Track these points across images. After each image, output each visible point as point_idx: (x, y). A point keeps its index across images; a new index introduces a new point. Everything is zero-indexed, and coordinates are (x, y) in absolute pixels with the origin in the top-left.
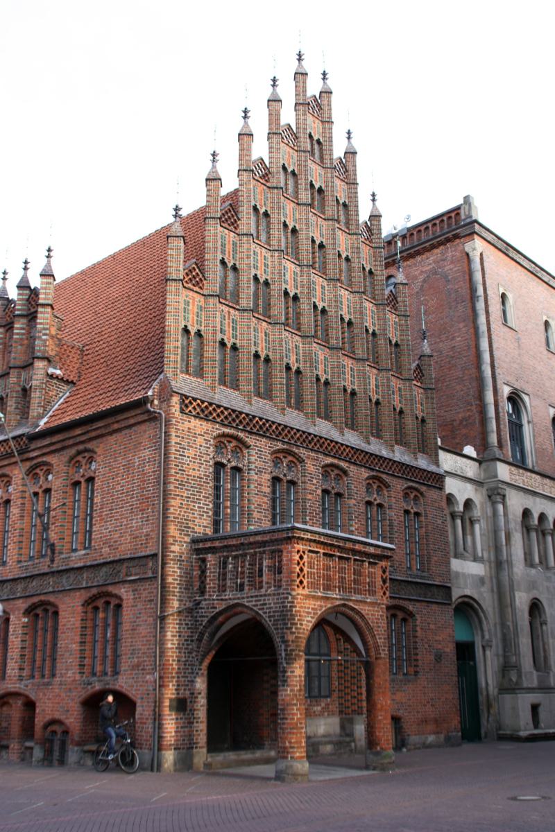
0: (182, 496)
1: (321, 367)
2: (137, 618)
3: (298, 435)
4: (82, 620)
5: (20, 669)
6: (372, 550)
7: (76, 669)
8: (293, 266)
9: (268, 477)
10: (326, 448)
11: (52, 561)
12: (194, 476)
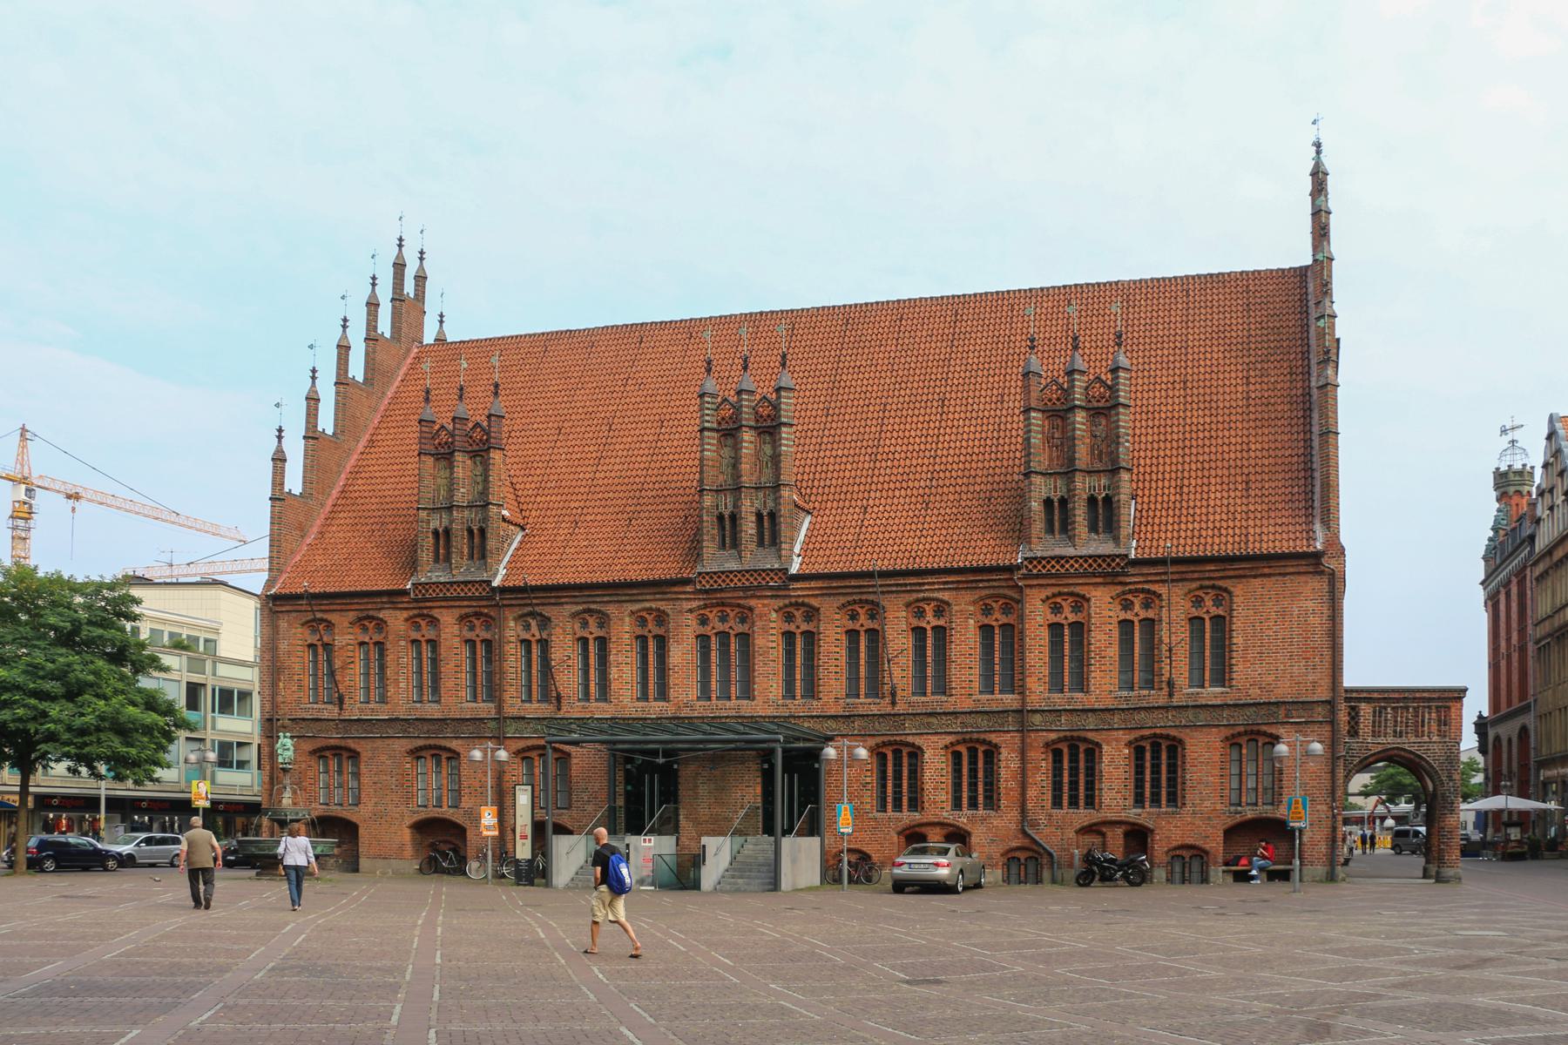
11: (1171, 695)
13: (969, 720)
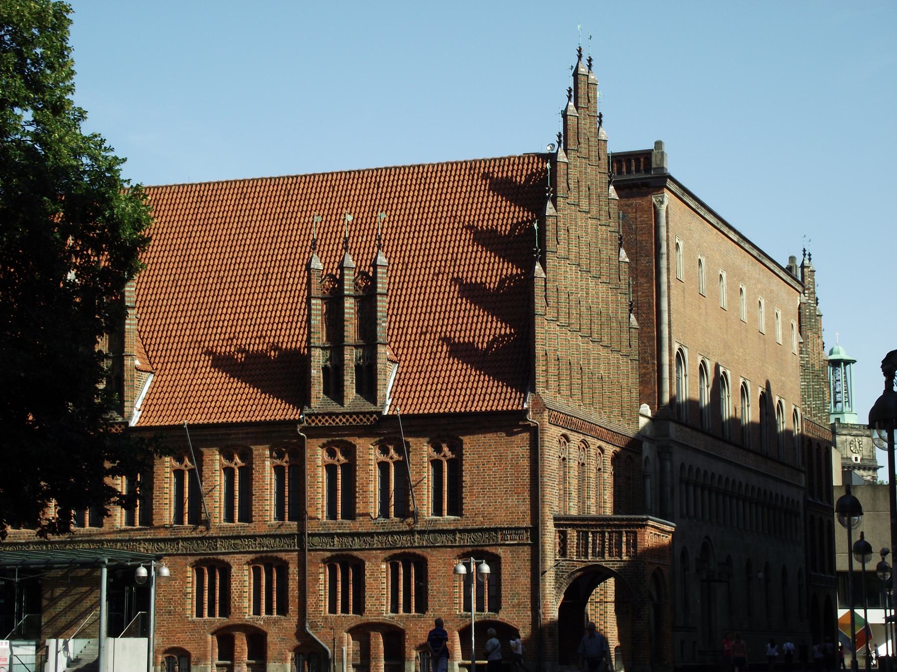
13: (266, 541)
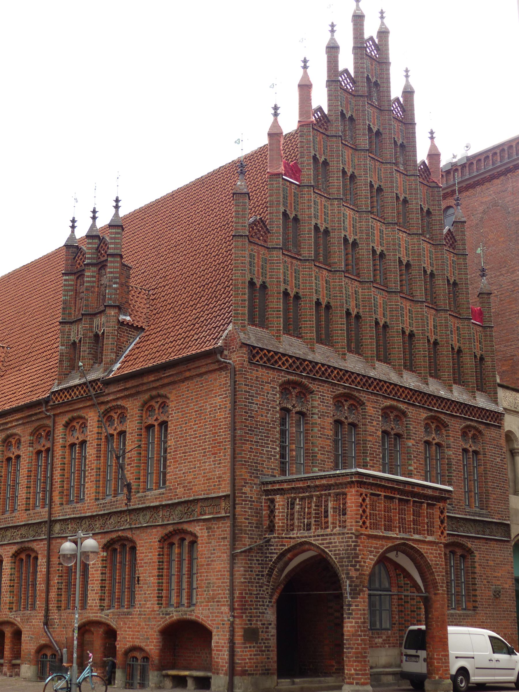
0: (252, 441)
1: (380, 310)
2: (212, 554)
3: (358, 379)
4: (159, 555)
5: (101, 600)
6: (430, 492)
7: (155, 601)
8: (352, 213)
9: (331, 420)
10: (386, 390)
11: (129, 500)
12: (262, 422)
13: (23, 531)
